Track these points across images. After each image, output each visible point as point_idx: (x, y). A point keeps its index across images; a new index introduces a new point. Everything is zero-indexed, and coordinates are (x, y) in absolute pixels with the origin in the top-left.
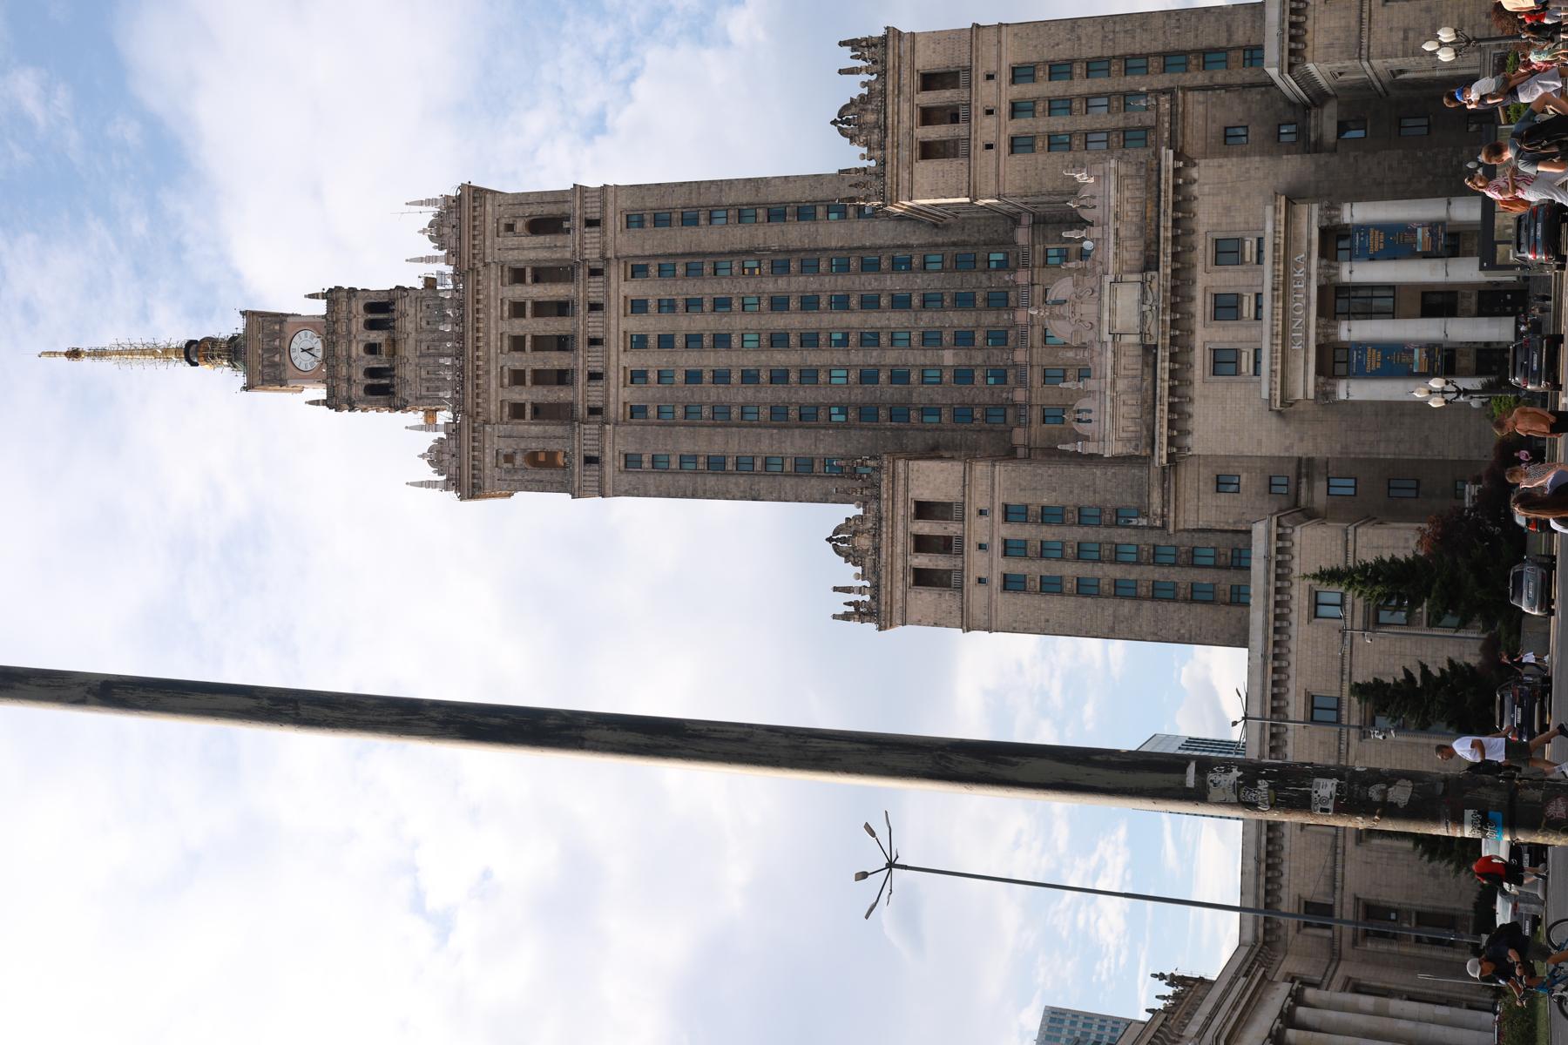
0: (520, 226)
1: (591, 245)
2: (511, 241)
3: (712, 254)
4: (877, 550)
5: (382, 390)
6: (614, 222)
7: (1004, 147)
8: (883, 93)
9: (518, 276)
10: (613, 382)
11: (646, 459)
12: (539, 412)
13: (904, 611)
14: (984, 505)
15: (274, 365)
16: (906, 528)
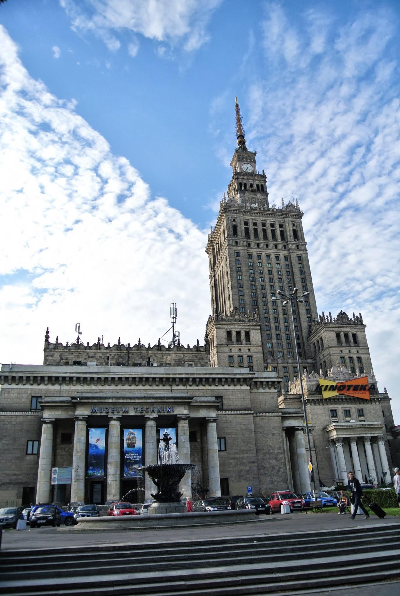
0: (295, 228)
1: (292, 246)
2: (291, 225)
3: (294, 278)
4: (235, 321)
5: (242, 188)
6: (299, 253)
7: (342, 355)
8: (351, 324)
9: (281, 226)
10: (257, 250)
11: (239, 258)
12: (247, 230)
13: (220, 328)
14: (252, 350)
15: (243, 159)
16: (242, 329)
